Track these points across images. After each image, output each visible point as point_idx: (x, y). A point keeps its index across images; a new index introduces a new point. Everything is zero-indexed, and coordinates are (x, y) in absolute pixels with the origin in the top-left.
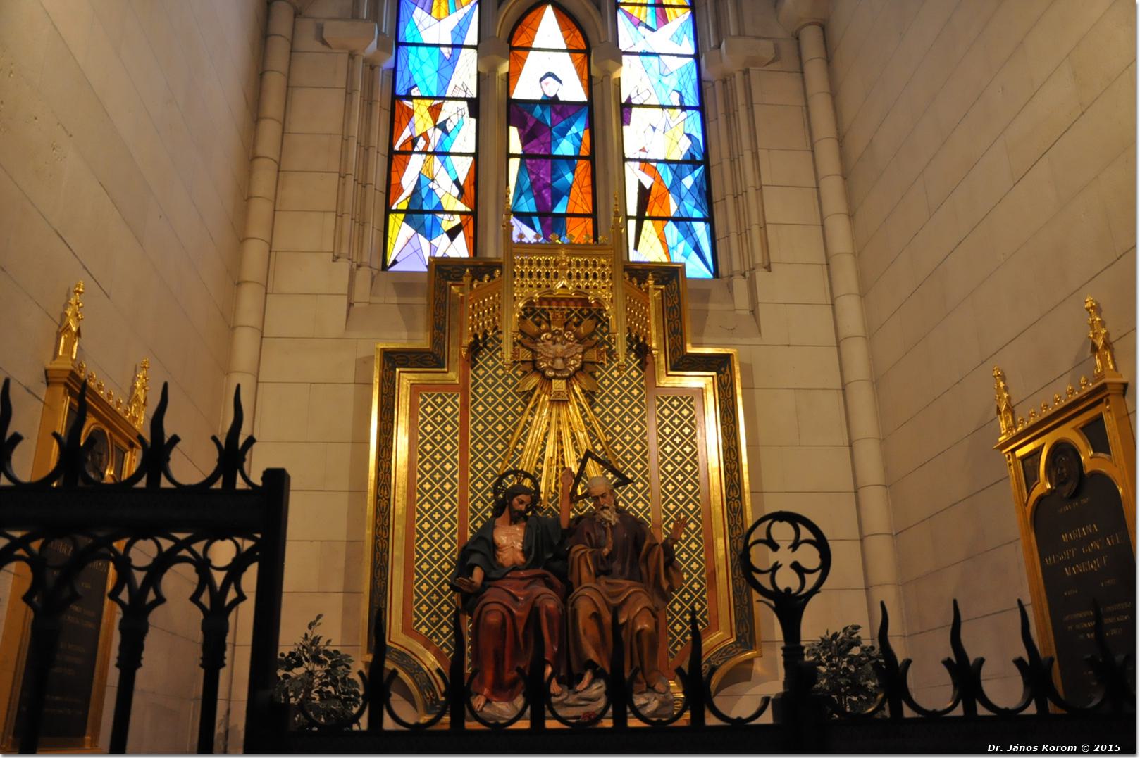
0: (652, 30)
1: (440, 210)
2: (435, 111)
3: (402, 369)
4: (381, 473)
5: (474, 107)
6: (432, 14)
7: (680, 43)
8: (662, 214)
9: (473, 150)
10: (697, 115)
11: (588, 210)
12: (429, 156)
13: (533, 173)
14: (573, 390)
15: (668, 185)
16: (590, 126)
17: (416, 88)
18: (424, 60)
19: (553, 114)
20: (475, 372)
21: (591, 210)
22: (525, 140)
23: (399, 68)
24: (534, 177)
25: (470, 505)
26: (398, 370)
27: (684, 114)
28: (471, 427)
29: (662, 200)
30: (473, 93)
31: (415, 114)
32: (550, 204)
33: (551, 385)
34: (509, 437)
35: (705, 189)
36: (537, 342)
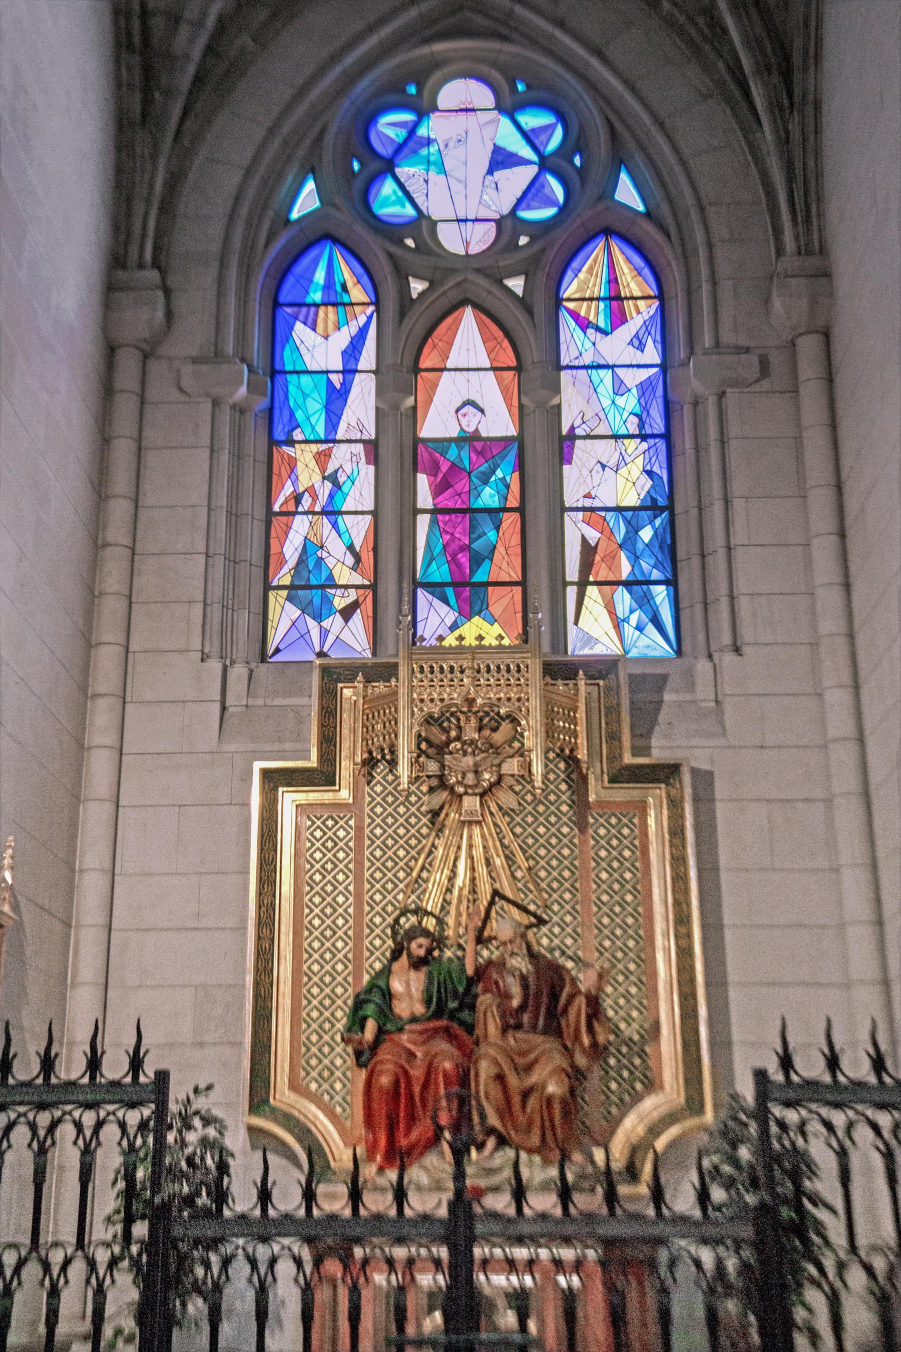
0: (605, 333)
1: (331, 583)
2: (322, 459)
3: (285, 789)
4: (263, 909)
5: (373, 450)
6: (318, 329)
7: (641, 347)
8: (611, 578)
9: (370, 507)
10: (661, 444)
11: (516, 576)
12: (316, 517)
13: (447, 532)
14: (489, 807)
15: (619, 540)
16: (520, 466)
17: (299, 430)
18: (307, 392)
19: (472, 455)
20: (372, 789)
21: (520, 576)
22: (437, 491)
23: (276, 405)
24: (448, 537)
25: (367, 942)
26: (281, 789)
27: (645, 445)
28: (367, 853)
29: (612, 561)
30: (370, 433)
31: (299, 463)
32: (468, 571)
33: (461, 801)
34: (412, 863)
35: (669, 542)
36: (445, 753)
